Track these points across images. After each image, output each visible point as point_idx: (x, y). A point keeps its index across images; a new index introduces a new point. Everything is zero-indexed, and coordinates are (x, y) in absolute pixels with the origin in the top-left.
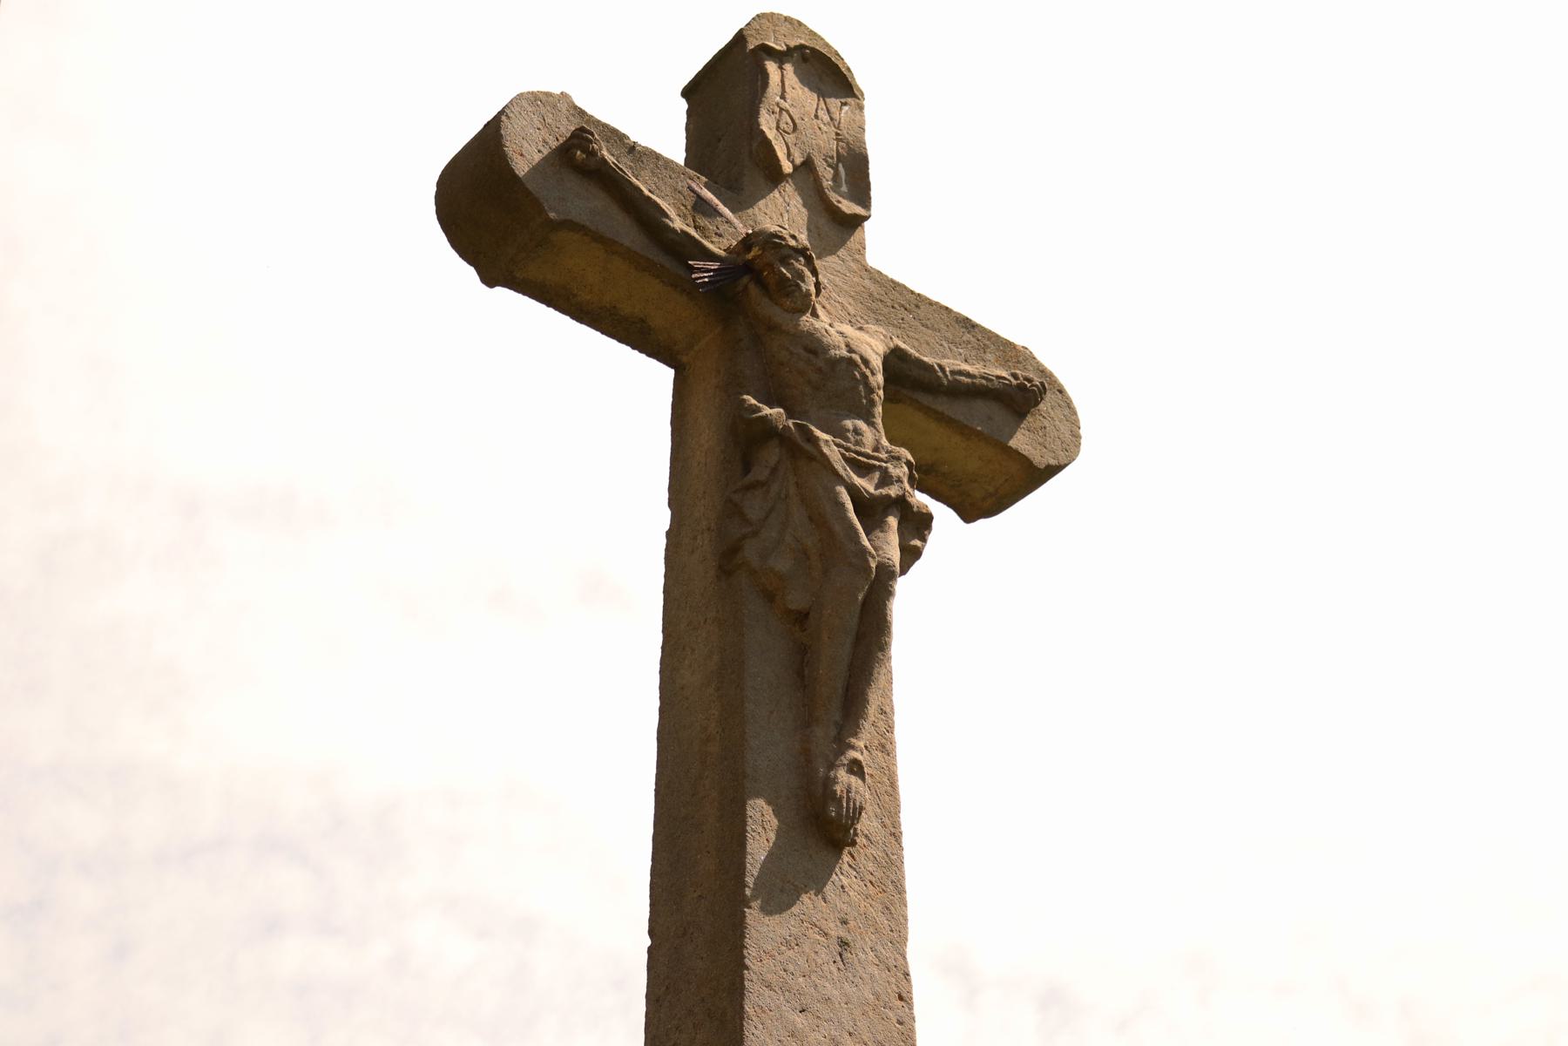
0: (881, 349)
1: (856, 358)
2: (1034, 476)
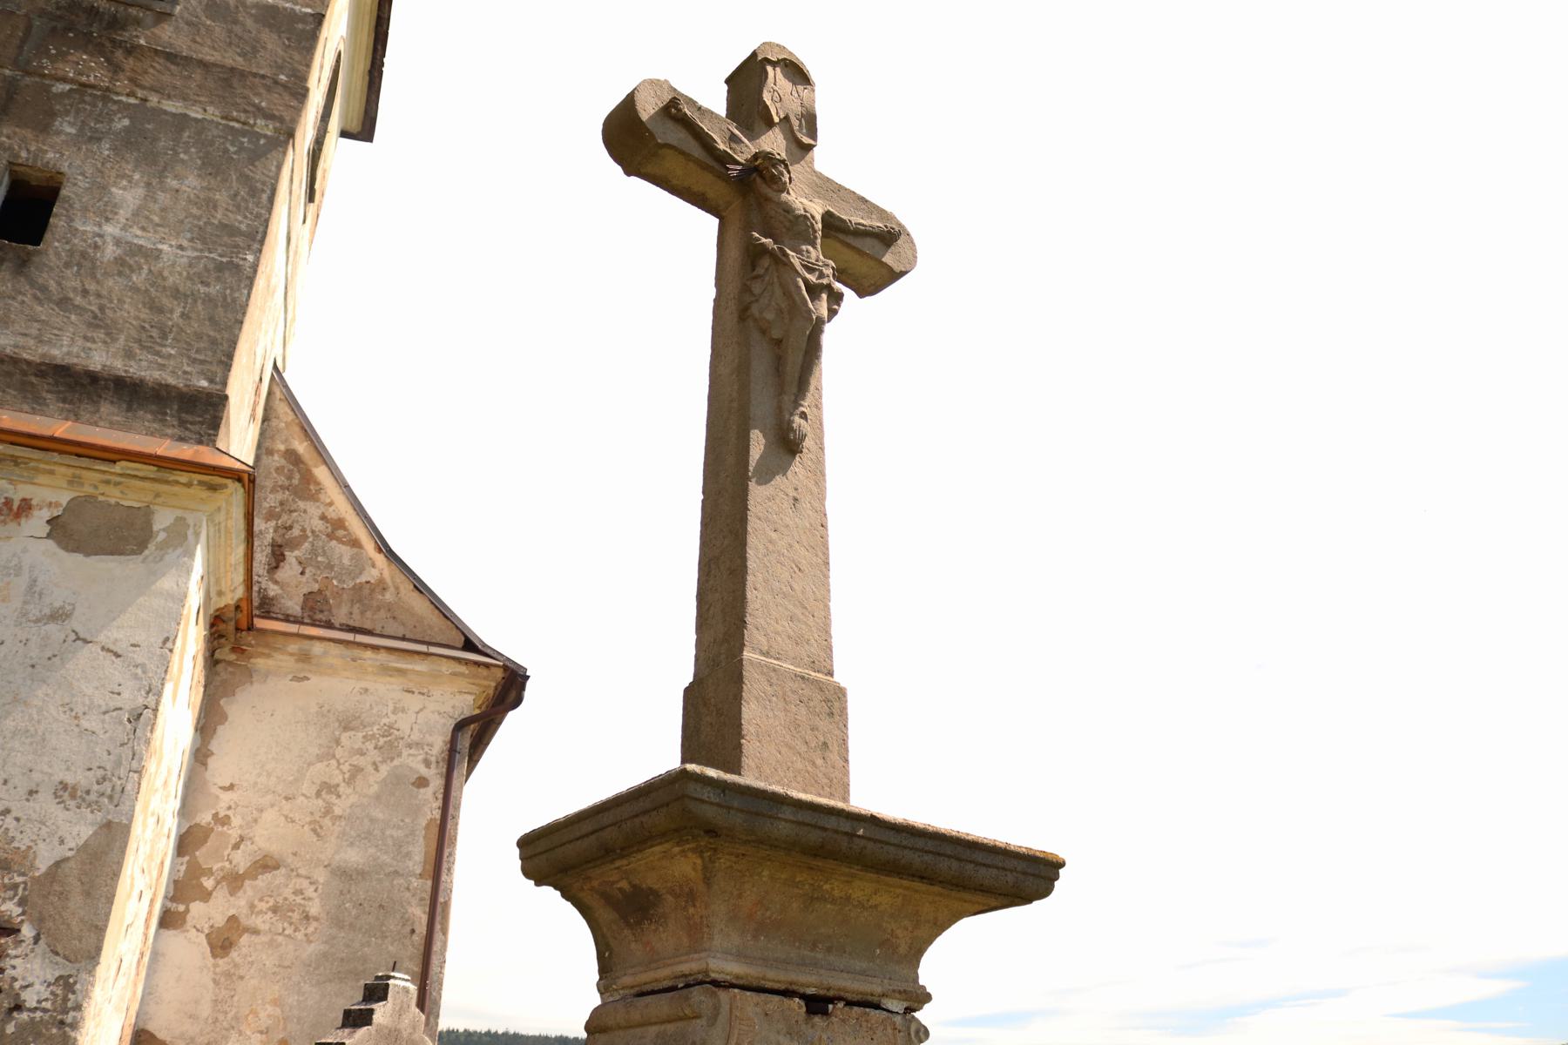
0: (821, 211)
1: (809, 215)
2: (894, 276)
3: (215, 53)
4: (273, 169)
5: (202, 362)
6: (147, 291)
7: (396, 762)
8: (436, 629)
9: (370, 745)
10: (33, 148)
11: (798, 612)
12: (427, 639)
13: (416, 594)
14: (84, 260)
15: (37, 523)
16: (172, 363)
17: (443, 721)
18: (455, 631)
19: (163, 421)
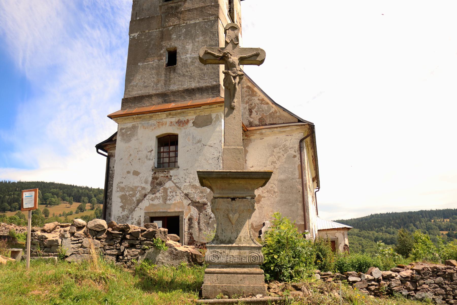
3: (197, 5)
4: (217, 27)
5: (213, 78)
6: (199, 67)
7: (288, 153)
8: (291, 119)
9: (281, 150)
10: (169, 44)
11: (235, 137)
12: (289, 122)
13: (284, 112)
14: (185, 65)
15: (191, 124)
16: (207, 81)
17: (297, 141)
18: (295, 119)
19: (209, 94)
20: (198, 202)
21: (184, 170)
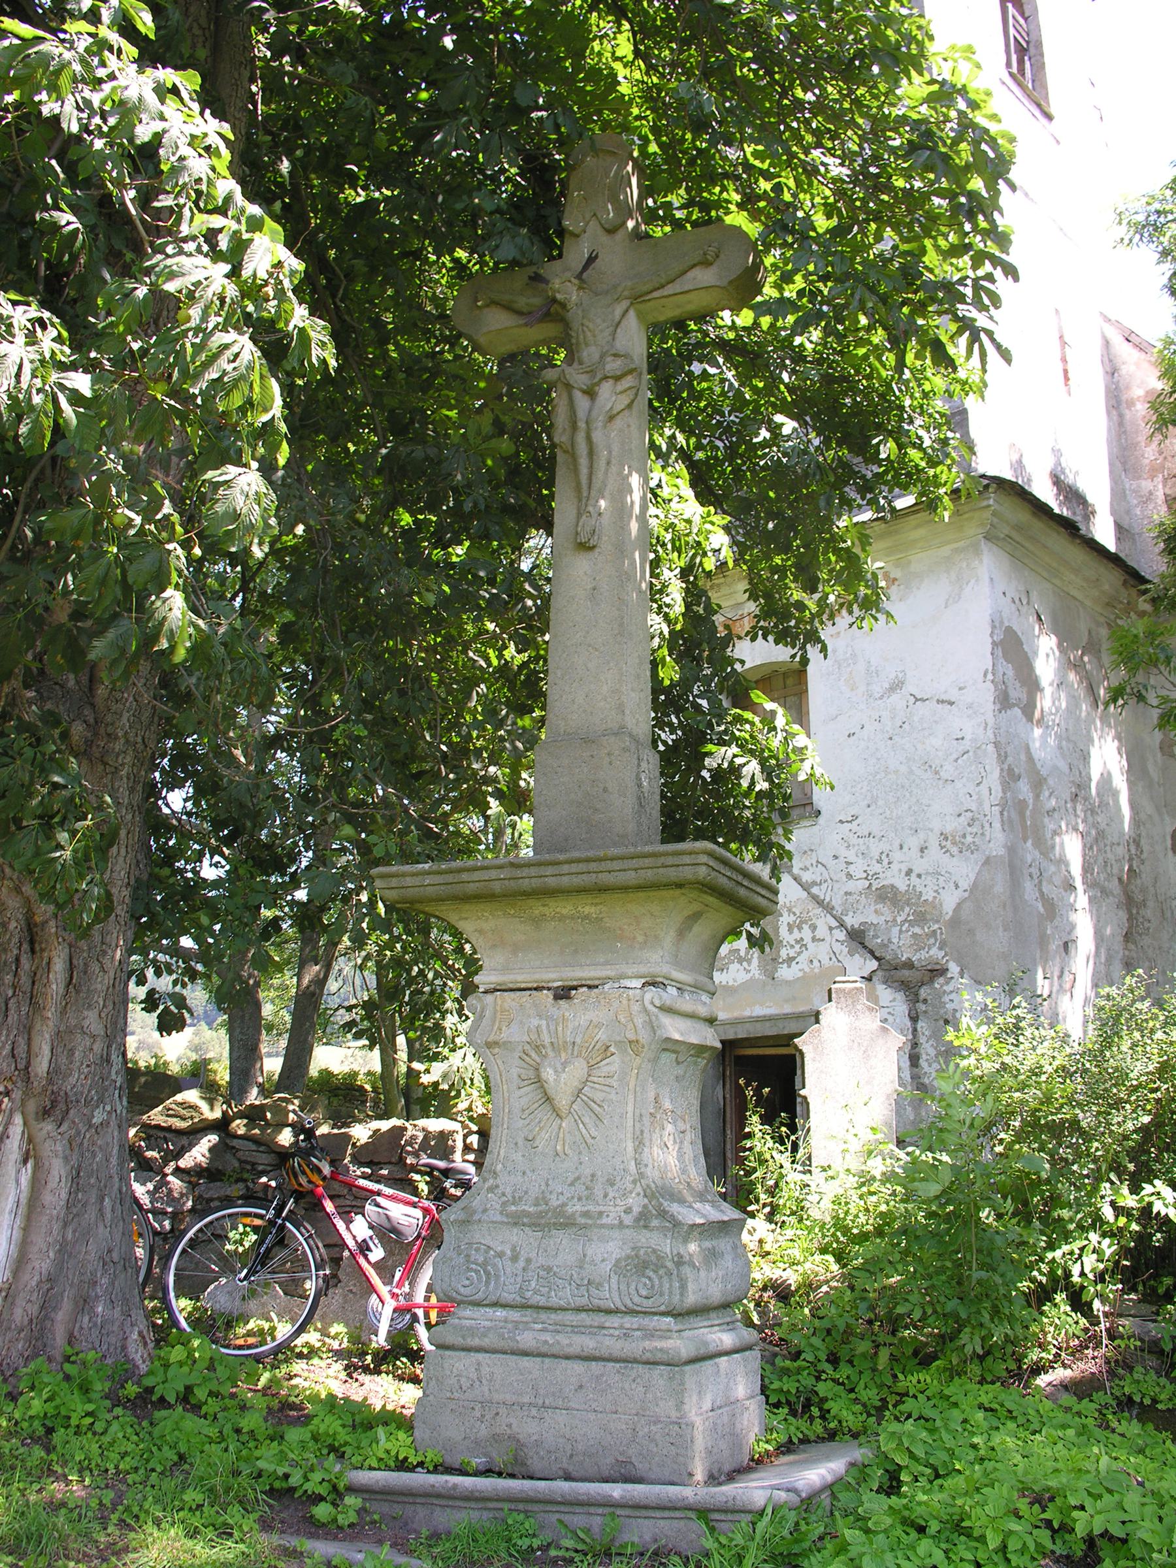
20: (909, 965)
21: (841, 822)
